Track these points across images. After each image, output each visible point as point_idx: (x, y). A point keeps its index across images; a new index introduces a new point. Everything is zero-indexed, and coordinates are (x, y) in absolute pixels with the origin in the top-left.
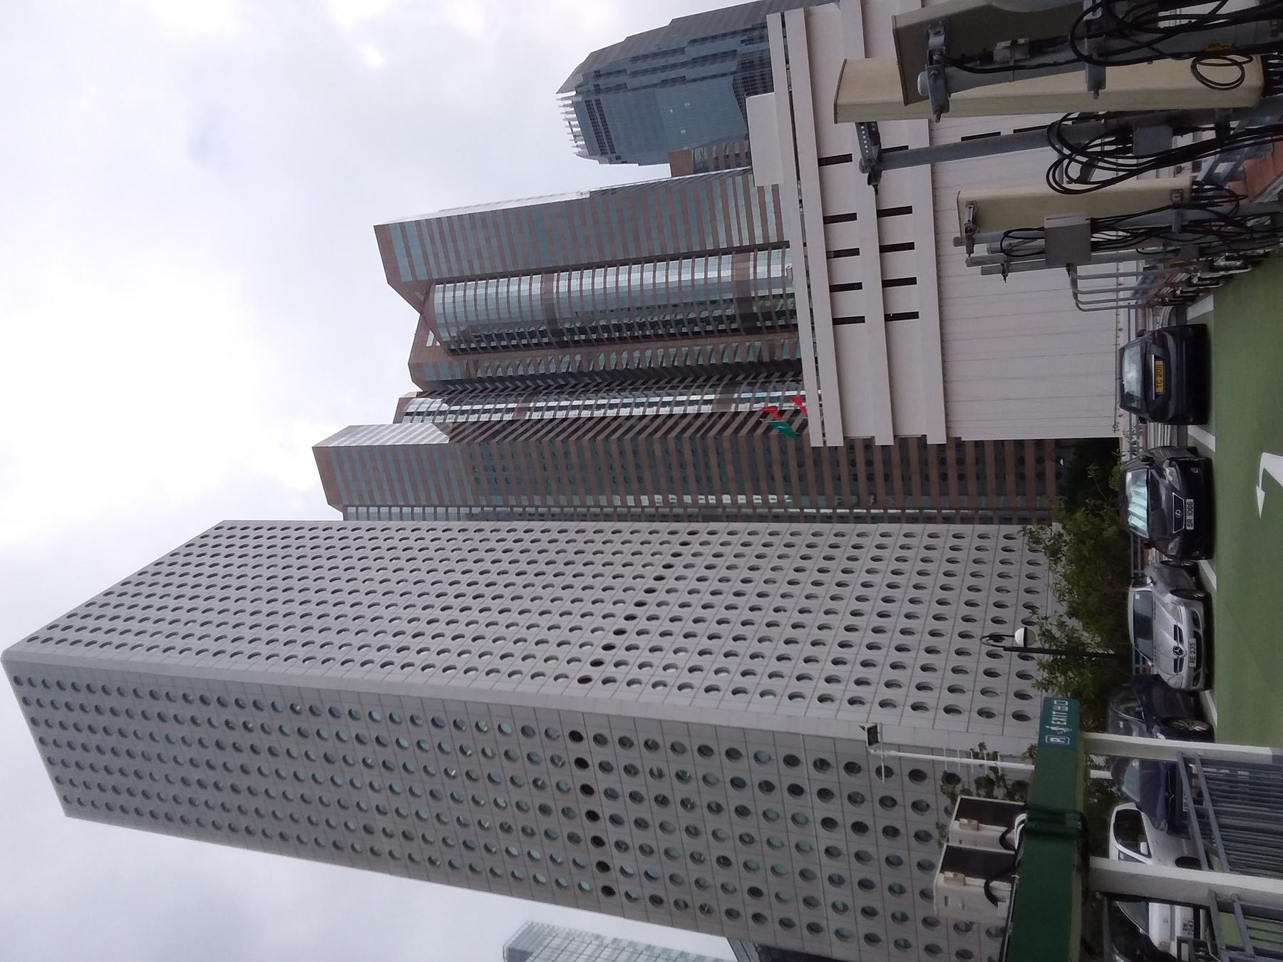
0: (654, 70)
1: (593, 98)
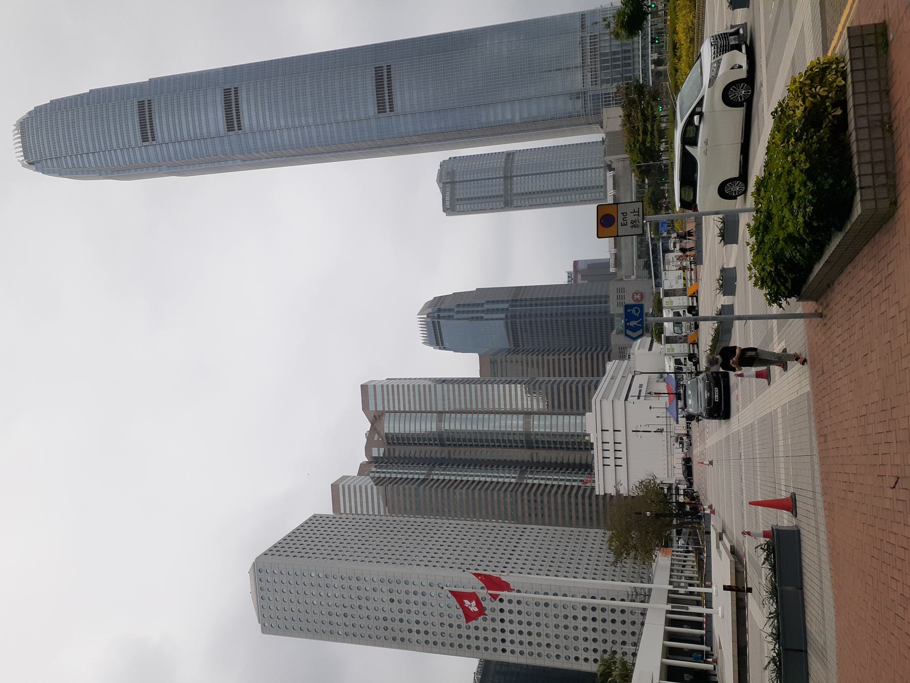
0: (468, 312)
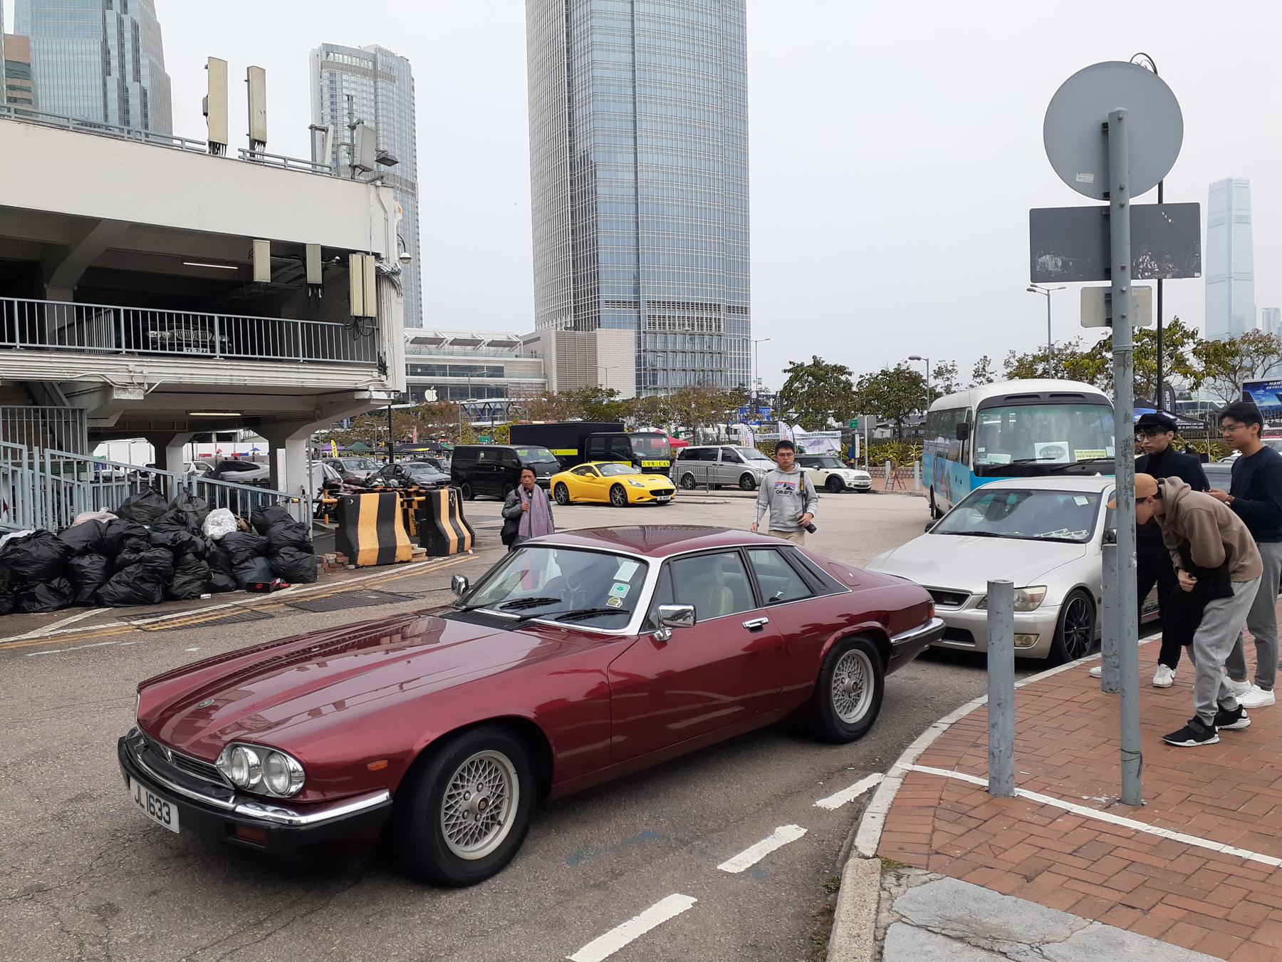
0: (121, 45)
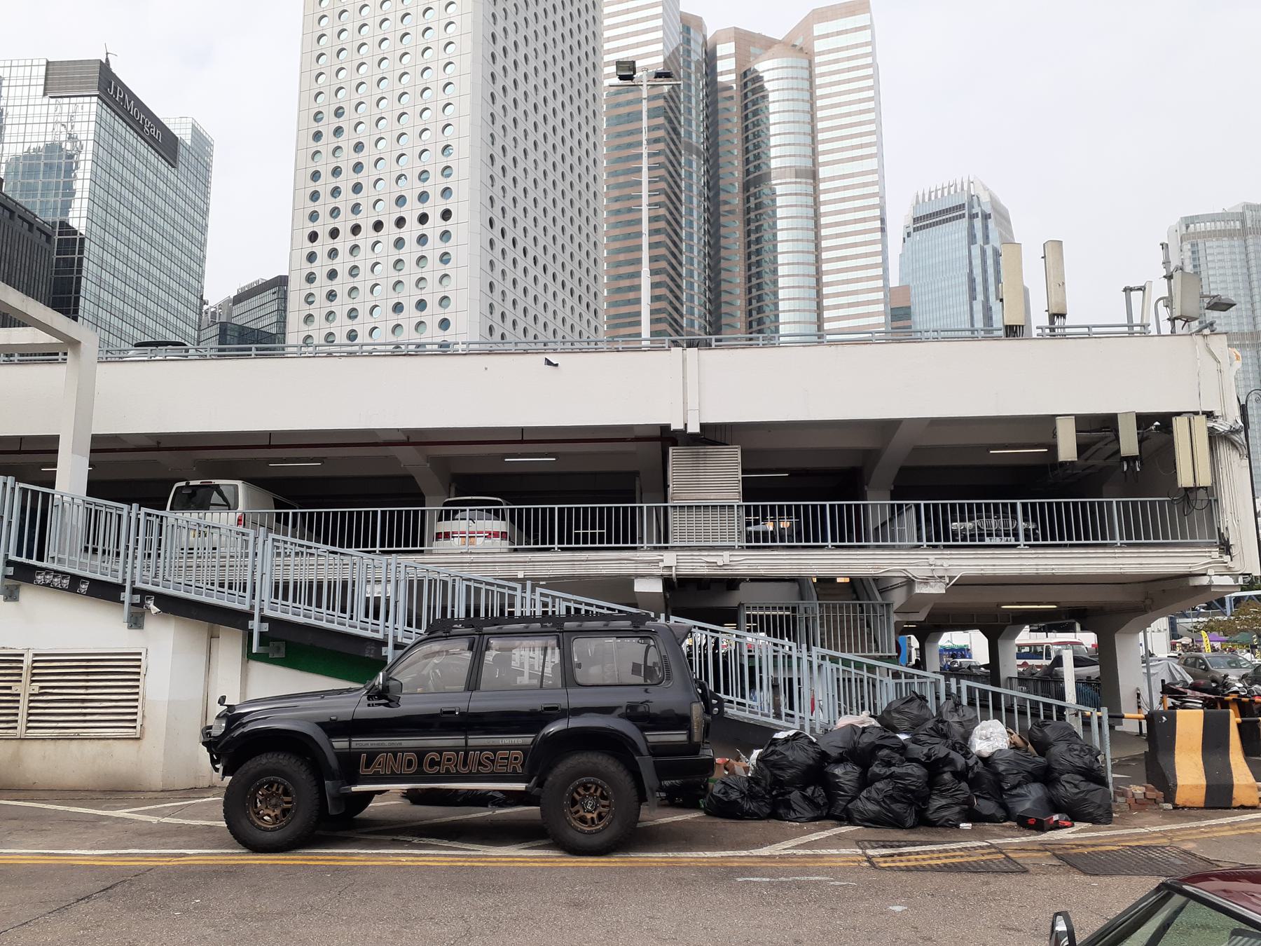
0: (985, 271)
1: (966, 212)
